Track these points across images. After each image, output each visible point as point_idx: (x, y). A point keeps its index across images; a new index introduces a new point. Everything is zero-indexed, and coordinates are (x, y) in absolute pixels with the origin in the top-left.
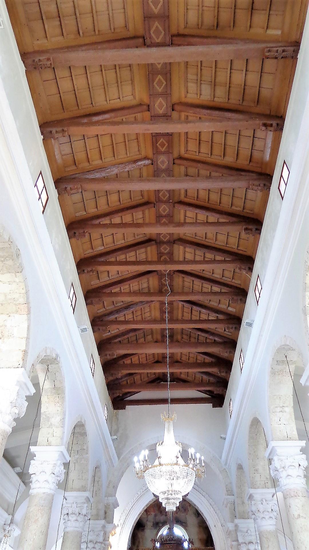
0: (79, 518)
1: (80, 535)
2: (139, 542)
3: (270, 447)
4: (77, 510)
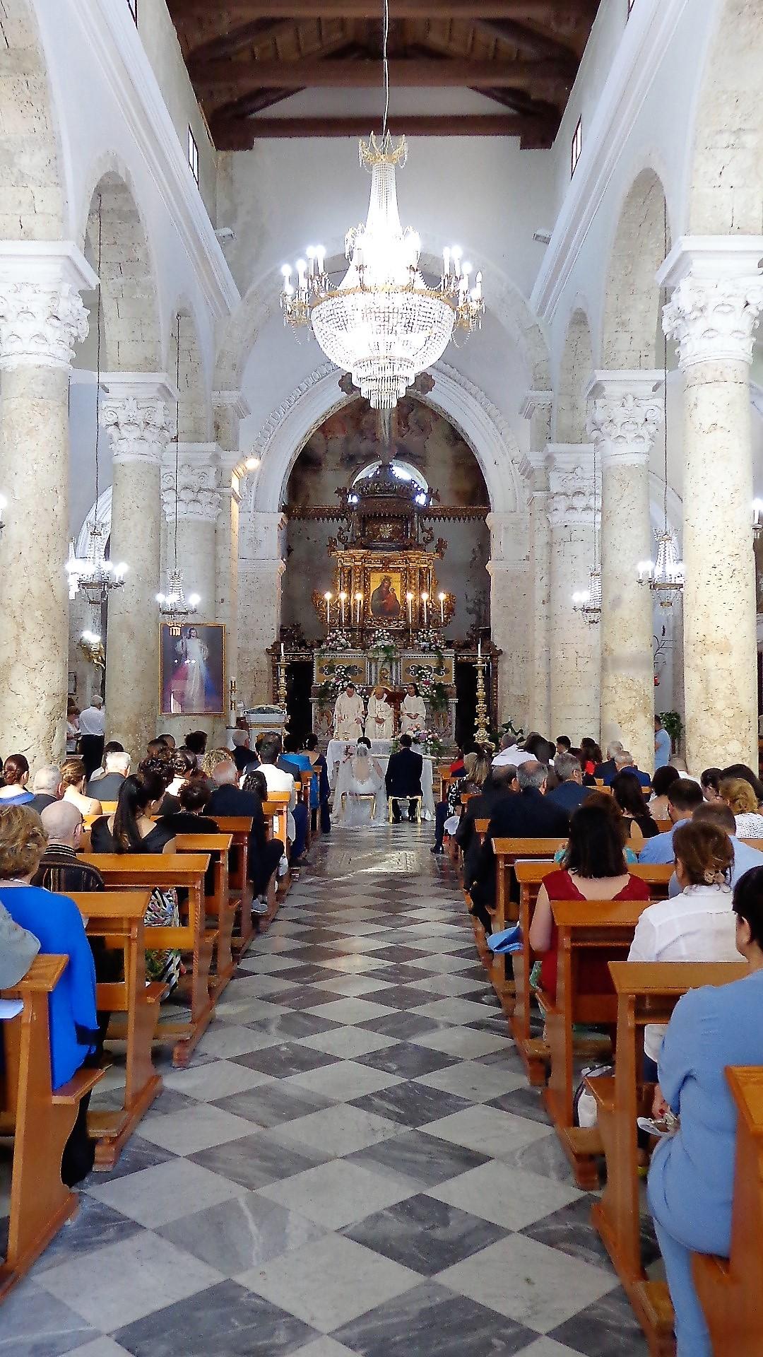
0: (147, 434)
1: (155, 472)
2: (308, 496)
3: (674, 255)
4: (140, 417)
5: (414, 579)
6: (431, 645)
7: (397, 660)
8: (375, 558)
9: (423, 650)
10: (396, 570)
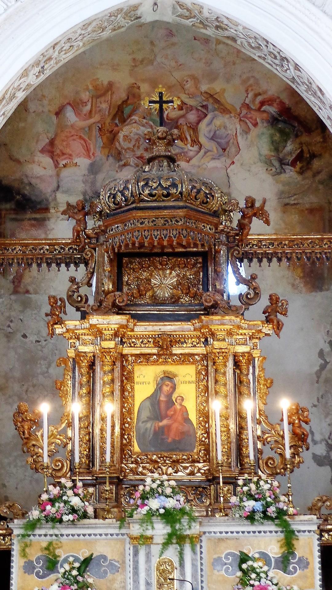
5: (224, 374)
6: (268, 505)
7: (194, 540)
8: (143, 337)
9: (251, 517)
10: (186, 359)
